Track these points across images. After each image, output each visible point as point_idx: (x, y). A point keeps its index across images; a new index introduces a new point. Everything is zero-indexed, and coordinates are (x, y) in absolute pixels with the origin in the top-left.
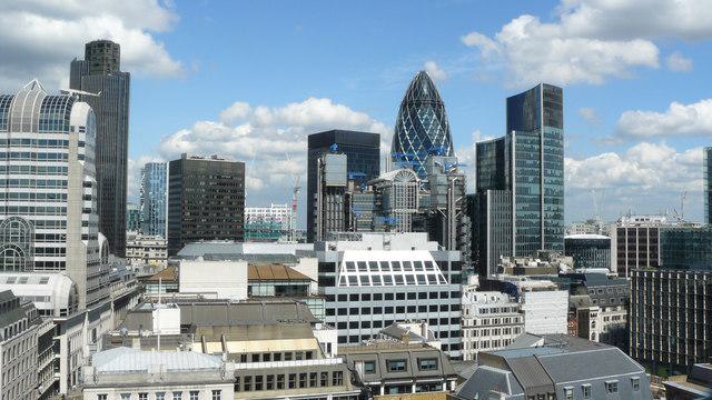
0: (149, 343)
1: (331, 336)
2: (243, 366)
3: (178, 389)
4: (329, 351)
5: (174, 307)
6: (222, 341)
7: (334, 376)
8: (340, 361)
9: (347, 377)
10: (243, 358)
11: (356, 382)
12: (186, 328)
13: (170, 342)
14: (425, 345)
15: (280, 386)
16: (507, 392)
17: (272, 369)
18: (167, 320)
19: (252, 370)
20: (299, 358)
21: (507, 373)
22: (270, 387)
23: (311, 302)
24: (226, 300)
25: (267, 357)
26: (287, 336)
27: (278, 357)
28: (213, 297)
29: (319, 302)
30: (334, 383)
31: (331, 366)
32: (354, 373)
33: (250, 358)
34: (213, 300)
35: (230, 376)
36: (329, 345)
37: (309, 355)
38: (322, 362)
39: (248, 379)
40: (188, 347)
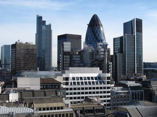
0: (9, 105)
1: (68, 102)
2: (40, 112)
4: (68, 107)
5: (16, 93)
7: (70, 114)
8: (72, 110)
10: (40, 110)
13: (16, 104)
14: (99, 105)
17: (49, 113)
18: (14, 97)
19: (54, 112)
21: (128, 114)
25: (48, 109)
26: (54, 102)
27: (51, 109)
28: (29, 89)
31: (69, 111)
33: (42, 109)
34: (29, 90)
36: (68, 104)
37: (62, 108)
38: (66, 110)
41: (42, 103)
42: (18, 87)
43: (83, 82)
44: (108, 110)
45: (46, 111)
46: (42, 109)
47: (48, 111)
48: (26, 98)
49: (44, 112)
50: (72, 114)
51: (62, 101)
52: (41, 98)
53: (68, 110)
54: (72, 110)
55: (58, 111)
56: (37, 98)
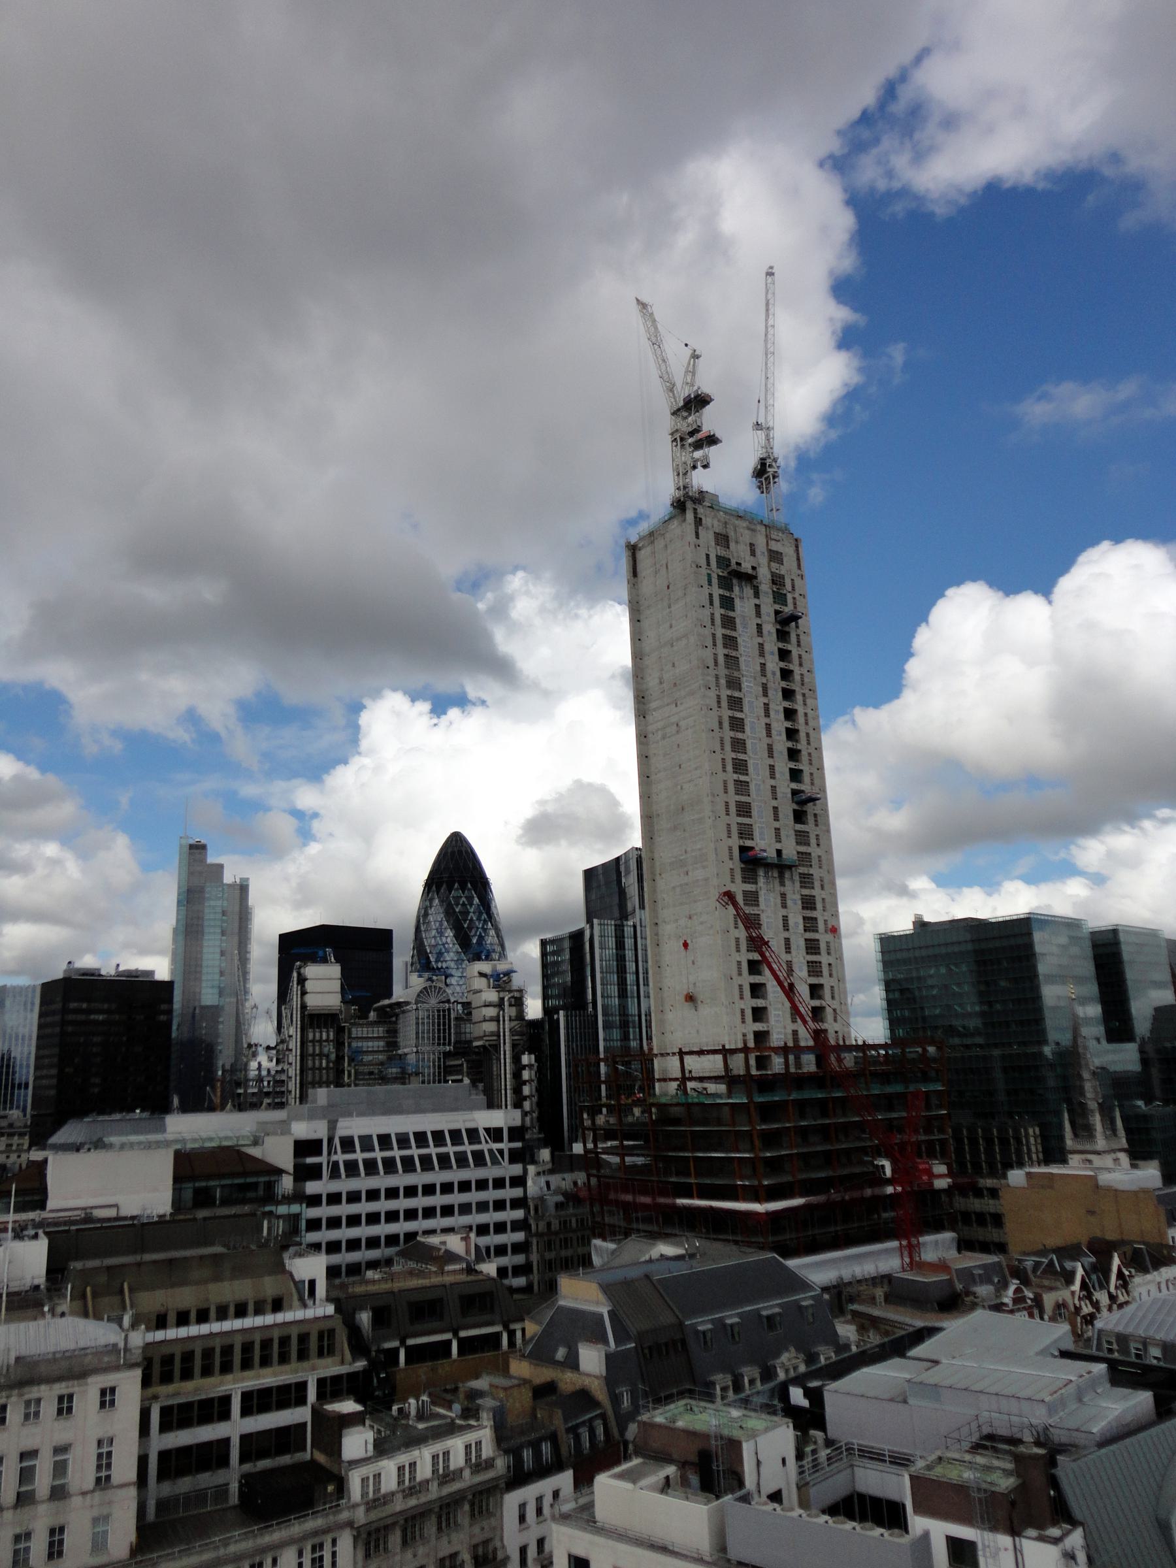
1: (311, 1268)
2: (160, 1335)
3: (34, 1392)
5: (36, 1237)
6: (122, 1292)
9: (342, 1338)
11: (359, 1346)
12: (56, 1269)
14: (470, 1270)
15: (226, 1368)
16: (605, 1341)
20: (258, 1311)
22: (207, 1372)
23: (282, 1210)
24: (133, 1218)
26: (240, 1271)
28: (112, 1213)
29: (295, 1208)
30: (321, 1354)
32: (354, 1331)
33: (172, 1318)
34: (109, 1220)
35: (137, 1356)
36: (312, 1283)
37: (278, 1305)
39: (168, 1360)
40: (59, 1310)
41: (173, 1286)
42: (50, 1204)
43: (356, 1161)
44: (516, 1296)
45: (194, 1330)
46: (172, 1318)
47: (204, 1329)
48: (90, 1260)
49: (183, 1332)
50: (331, 1332)
51: (280, 1268)
52: (171, 1261)
53: (310, 1313)
54: (330, 1309)
55: (259, 1321)
56: (148, 1257)
